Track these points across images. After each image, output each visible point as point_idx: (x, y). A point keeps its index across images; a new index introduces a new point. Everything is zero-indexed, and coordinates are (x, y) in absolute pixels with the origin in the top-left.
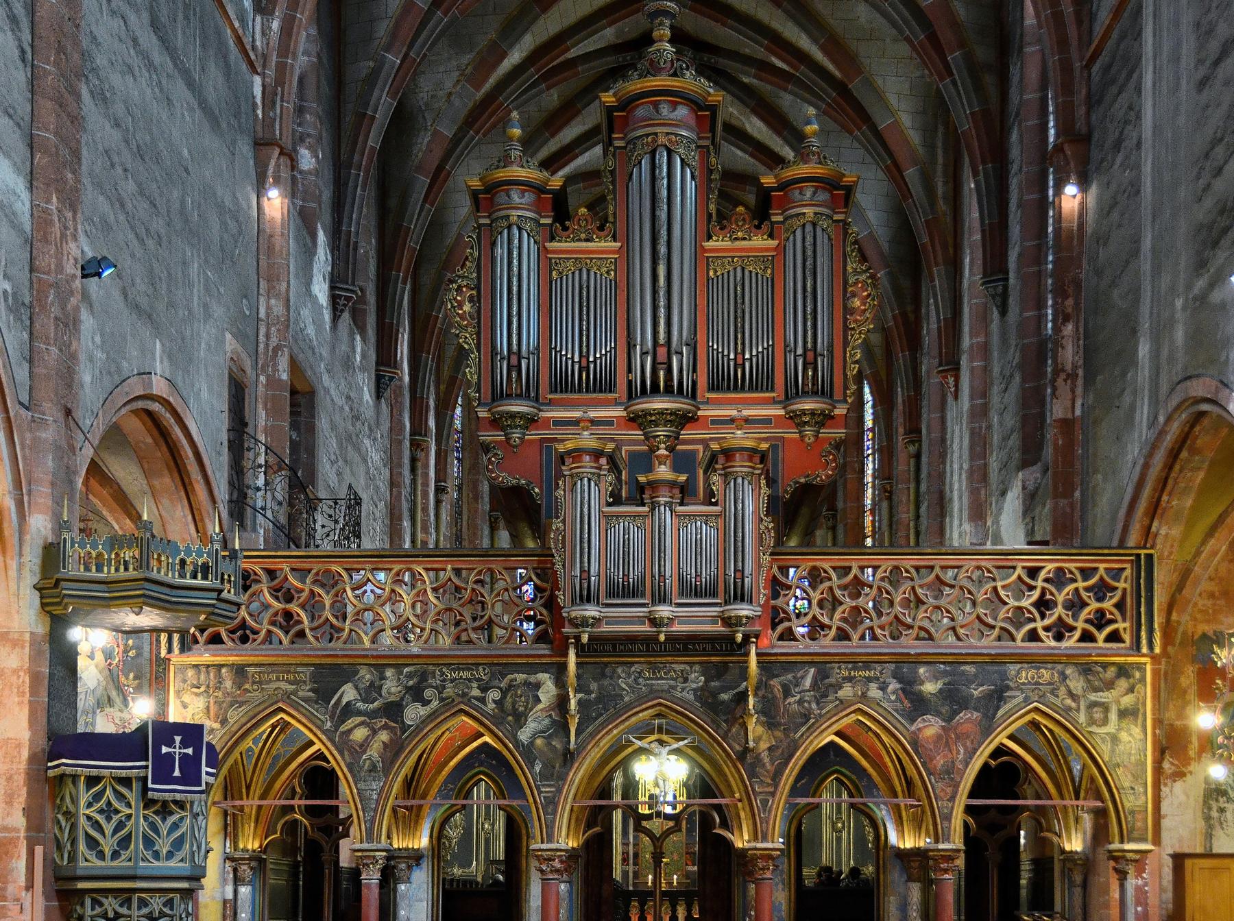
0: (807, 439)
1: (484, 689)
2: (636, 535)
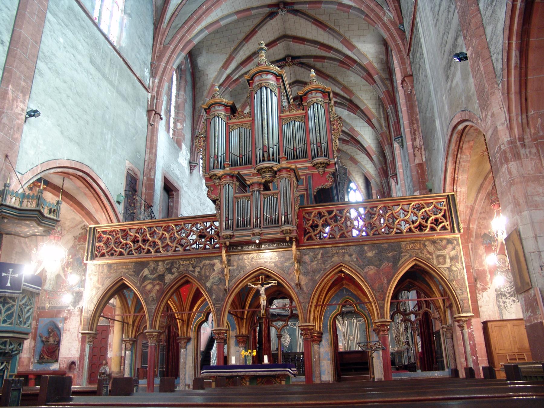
0: (320, 173)
1: (194, 267)
2: (247, 203)
